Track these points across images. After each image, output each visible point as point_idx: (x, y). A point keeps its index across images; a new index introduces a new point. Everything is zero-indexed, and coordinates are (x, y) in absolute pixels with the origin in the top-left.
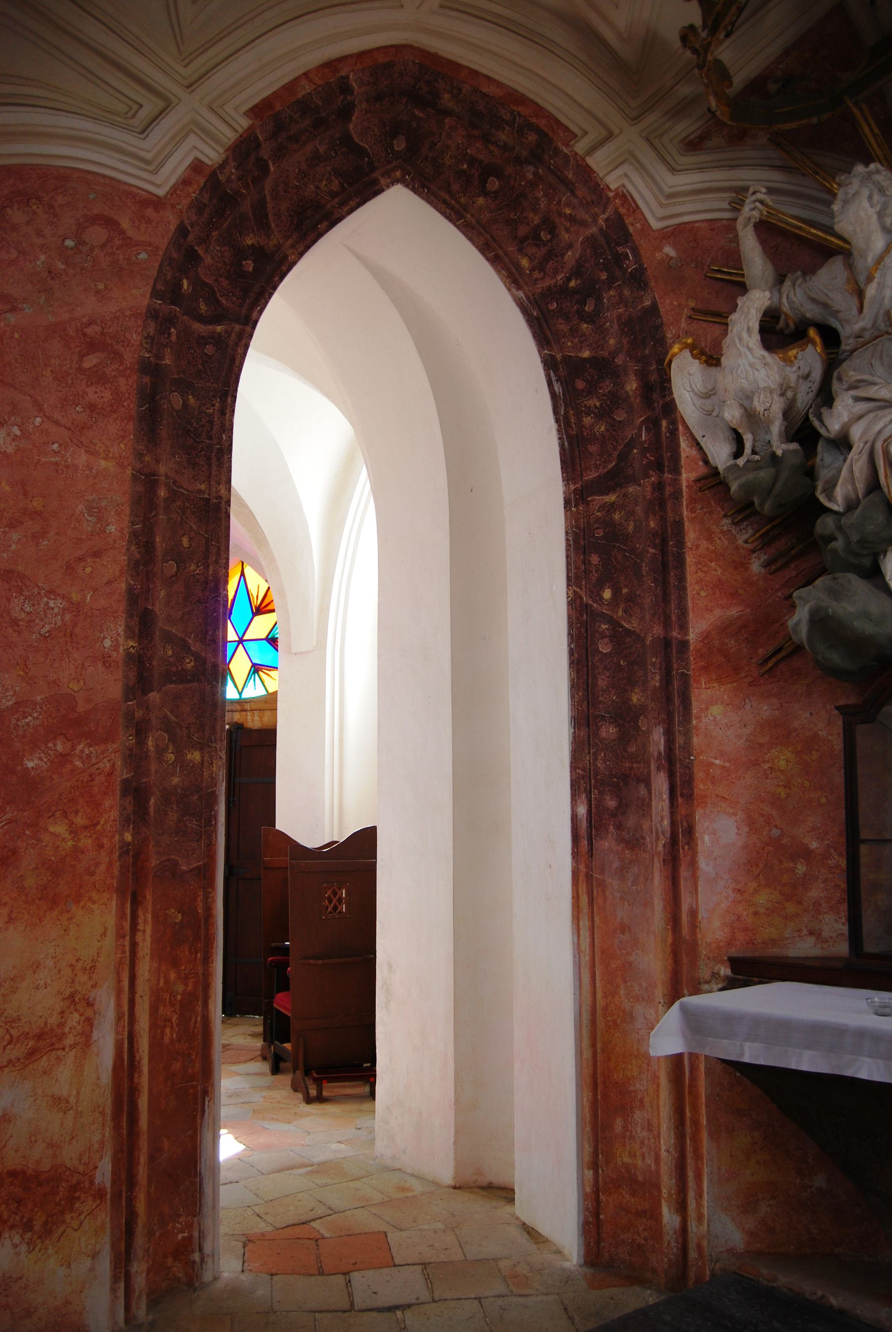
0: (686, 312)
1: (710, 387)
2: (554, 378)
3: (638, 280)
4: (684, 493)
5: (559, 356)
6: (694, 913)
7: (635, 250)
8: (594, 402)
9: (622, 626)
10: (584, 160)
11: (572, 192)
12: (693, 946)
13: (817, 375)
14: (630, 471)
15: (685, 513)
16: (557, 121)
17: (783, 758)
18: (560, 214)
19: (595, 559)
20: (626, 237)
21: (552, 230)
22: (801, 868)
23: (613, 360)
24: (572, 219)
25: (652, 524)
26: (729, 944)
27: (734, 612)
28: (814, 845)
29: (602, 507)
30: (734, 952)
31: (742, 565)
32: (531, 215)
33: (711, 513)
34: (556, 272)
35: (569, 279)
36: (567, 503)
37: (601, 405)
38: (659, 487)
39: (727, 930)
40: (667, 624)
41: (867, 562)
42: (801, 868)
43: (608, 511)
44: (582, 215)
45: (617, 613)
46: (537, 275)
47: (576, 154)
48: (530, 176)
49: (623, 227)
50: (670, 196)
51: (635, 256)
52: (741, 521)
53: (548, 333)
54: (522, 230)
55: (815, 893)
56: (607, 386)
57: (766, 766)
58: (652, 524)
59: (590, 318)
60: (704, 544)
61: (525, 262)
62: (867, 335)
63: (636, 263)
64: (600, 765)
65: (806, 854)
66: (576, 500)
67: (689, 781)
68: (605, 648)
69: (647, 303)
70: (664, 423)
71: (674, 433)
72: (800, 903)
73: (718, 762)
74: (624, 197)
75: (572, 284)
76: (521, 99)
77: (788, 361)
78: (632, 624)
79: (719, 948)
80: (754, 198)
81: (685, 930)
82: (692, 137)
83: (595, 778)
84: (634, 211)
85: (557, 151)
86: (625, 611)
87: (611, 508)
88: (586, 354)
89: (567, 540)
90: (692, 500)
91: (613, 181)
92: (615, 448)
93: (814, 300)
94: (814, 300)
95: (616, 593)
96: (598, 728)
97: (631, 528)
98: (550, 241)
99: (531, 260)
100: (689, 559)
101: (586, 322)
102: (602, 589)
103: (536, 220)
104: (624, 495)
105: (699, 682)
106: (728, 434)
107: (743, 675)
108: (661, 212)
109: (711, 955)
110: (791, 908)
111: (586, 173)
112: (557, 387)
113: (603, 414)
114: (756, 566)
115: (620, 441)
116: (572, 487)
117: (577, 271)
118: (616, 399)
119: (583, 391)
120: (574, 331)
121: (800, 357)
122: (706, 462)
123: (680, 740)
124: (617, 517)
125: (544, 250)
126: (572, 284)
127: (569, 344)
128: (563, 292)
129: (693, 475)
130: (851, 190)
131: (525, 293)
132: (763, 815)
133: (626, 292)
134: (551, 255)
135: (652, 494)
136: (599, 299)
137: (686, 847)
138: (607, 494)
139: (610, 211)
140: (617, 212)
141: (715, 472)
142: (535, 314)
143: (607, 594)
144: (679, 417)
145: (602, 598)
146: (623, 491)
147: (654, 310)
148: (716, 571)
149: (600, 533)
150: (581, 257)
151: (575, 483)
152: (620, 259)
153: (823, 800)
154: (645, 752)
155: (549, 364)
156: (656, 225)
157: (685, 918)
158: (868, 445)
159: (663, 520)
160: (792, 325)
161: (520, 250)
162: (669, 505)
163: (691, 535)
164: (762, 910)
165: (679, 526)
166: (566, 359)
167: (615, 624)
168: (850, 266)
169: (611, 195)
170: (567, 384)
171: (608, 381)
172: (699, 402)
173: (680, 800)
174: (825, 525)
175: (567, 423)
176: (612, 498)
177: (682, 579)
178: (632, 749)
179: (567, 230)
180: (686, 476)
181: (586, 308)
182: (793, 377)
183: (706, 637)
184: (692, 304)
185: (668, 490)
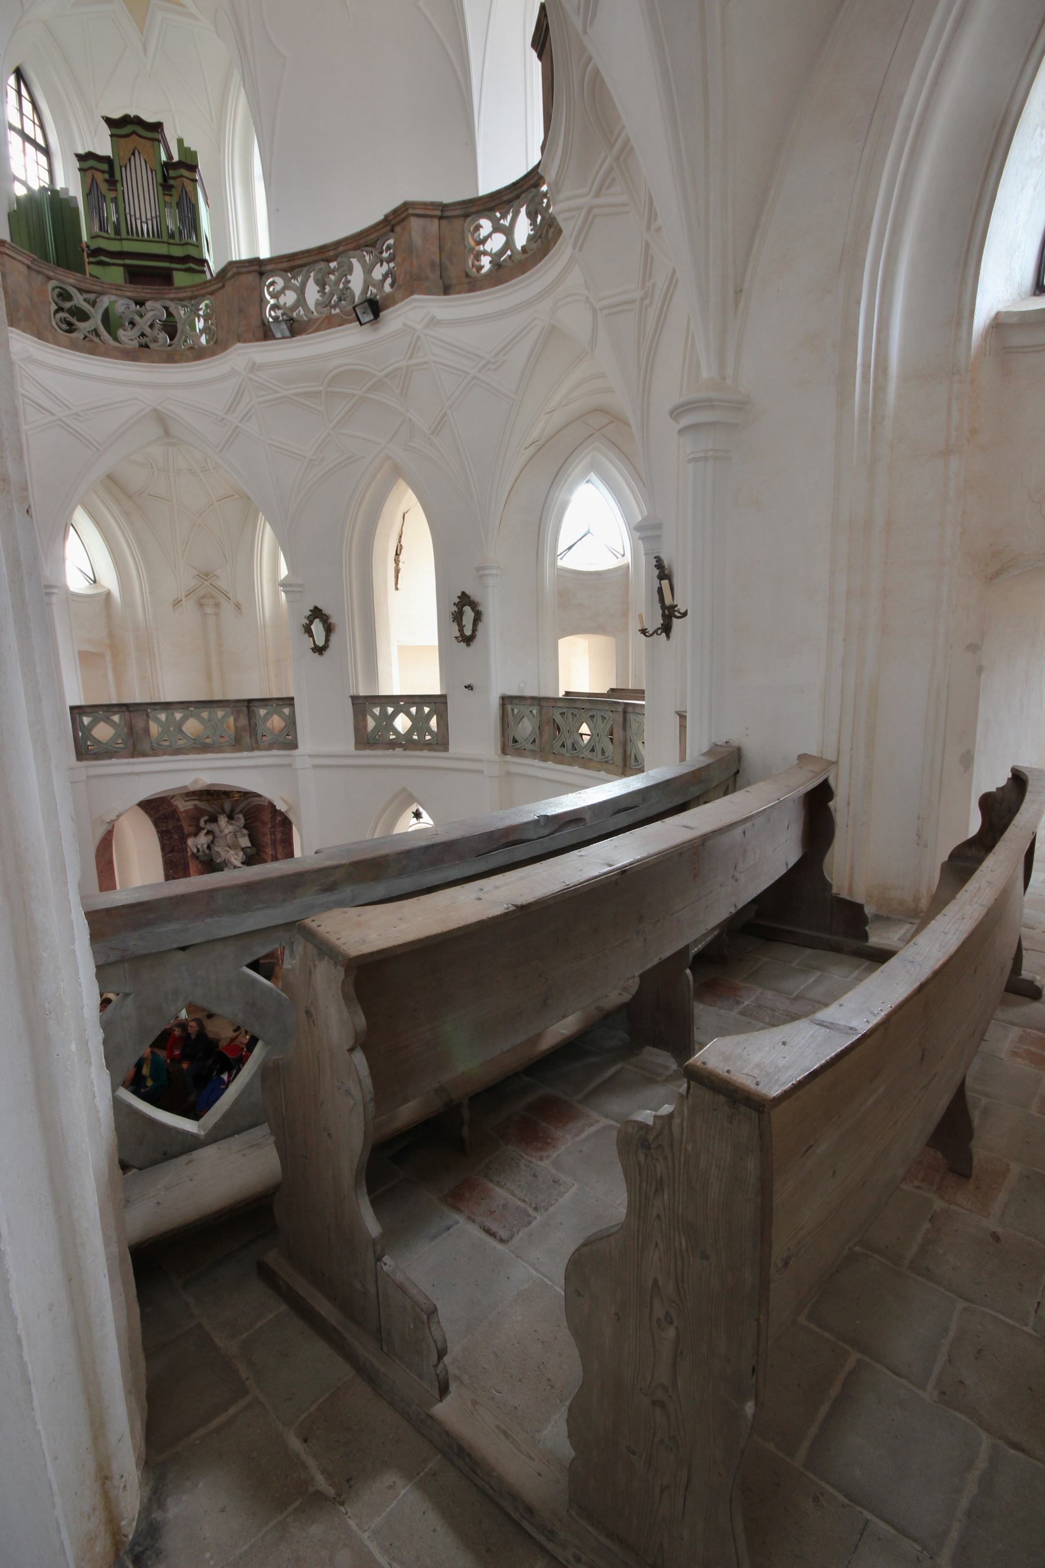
3: (178, 820)
7: (178, 815)
8: (166, 838)
13: (211, 839)
20: (176, 812)
59: (165, 823)
74: (176, 806)
87: (170, 857)
114: (200, 866)
143: (171, 872)
147: (182, 825)
155: (158, 832)
156: (181, 810)
163: (190, 864)
165: (188, 863)
170: (161, 835)
180: (189, 854)
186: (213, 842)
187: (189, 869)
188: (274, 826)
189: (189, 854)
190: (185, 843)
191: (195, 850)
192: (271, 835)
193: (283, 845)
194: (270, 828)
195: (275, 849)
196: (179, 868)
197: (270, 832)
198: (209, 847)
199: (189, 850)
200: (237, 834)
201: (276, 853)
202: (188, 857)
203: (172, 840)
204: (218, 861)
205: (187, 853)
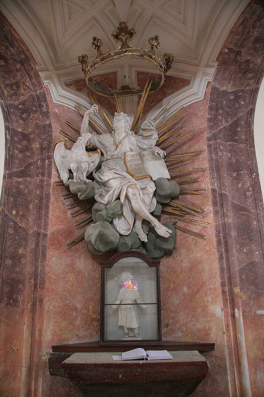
0: (59, 131)
1: (66, 156)
2: (7, 133)
4: (52, 186)
5: (11, 127)
6: (41, 331)
7: (47, 106)
8: (19, 146)
9: (18, 225)
10: (38, 72)
11: (30, 79)
12: (40, 343)
13: (97, 163)
14: (29, 173)
15: (51, 192)
16: (33, 57)
17: (71, 277)
18: (24, 84)
19: (11, 199)
20: (45, 100)
21: (18, 87)
22: (74, 314)
23: (29, 135)
24: (28, 87)
25: (38, 192)
26: (52, 341)
27: (61, 227)
28: (78, 306)
29: (16, 182)
30: (54, 344)
31: (66, 213)
32: (12, 79)
33: (58, 194)
34: (15, 101)
35: (19, 104)
36: (4, 177)
37: (22, 148)
38: (42, 181)
39: (52, 336)
40: (39, 227)
41: (110, 220)
42: (74, 314)
43: (18, 184)
44: (31, 87)
45: (17, 220)
46: (9, 98)
47: (36, 69)
48: (18, 67)
49: (45, 98)
50: (60, 95)
51: (46, 108)
52: (67, 199)
53: (9, 118)
54: (8, 82)
55: (78, 322)
56: (25, 143)
57: (67, 279)
58: (38, 192)
60: (56, 203)
61: (6, 92)
62: (115, 157)
63: (46, 110)
64: (4, 274)
65: (76, 309)
66: (8, 177)
67: (43, 283)
68: (11, 231)
69: (48, 123)
70: (47, 161)
71: (50, 165)
72: (73, 325)
73: (53, 277)
75: (20, 106)
76: (24, 44)
77: (90, 157)
78: (23, 225)
79: (49, 343)
80: (94, 108)
81: (37, 337)
82: (67, 83)
83: (2, 279)
84: (49, 95)
85: (30, 65)
86: (20, 220)
88: (20, 130)
89: (2, 190)
90: (53, 188)
91: (46, 82)
92: (24, 164)
93: (100, 142)
94: (100, 142)
95: (18, 212)
96: (5, 260)
97: (26, 191)
98: (16, 90)
99: (8, 92)
100: (51, 206)
101: (22, 120)
102: (12, 210)
103: (14, 81)
104: (25, 180)
105: (49, 248)
106: (68, 171)
107: (62, 248)
108: (57, 99)
109: (46, 346)
110: (71, 327)
111: (38, 76)
112: (8, 137)
113: (21, 151)
115: (26, 162)
116: (7, 172)
117: (23, 103)
118: (28, 148)
119: (16, 141)
120: (17, 121)
121: (93, 156)
122: (59, 177)
123: (40, 268)
124: (21, 186)
125: (13, 92)
126: (20, 106)
127: (15, 125)
128: (16, 107)
129: (55, 180)
130: (120, 118)
131: (4, 102)
132: (64, 296)
133: (40, 117)
134: (15, 94)
135: (39, 182)
136: (29, 115)
137: (40, 306)
138: (19, 178)
139: (42, 90)
140: (44, 92)
141: (62, 181)
142: (6, 110)
143: (14, 212)
144: (53, 161)
145: (12, 214)
146: (25, 179)
147: (50, 126)
148: (58, 213)
149: (14, 191)
150: (26, 100)
151: (9, 171)
152: (40, 106)
153: (81, 292)
154: (23, 271)
155: (7, 128)
157: (37, 333)
158: (122, 186)
159: (42, 192)
160: (91, 146)
161: (5, 88)
162: (45, 188)
163: (52, 199)
164: (62, 328)
165: (48, 196)
166: (13, 129)
167: (16, 223)
168: (113, 137)
169: (44, 86)
170: (12, 137)
171: (25, 142)
172: (61, 158)
173: (39, 289)
174: (96, 206)
175: (9, 150)
176: (20, 180)
177: (47, 213)
178: (17, 269)
179: (25, 90)
180: (54, 179)
181: (23, 116)
182: (90, 161)
183: (53, 234)
184: (61, 129)
185: (45, 183)
186: (99, 168)
187: (47, 207)
188: (214, 137)
189: (54, 179)
190: (50, 158)
191: (65, 176)
192: (210, 152)
193: (235, 175)
194: (209, 139)
195: (220, 178)
196: (31, 207)
197: (209, 146)
198: (90, 176)
199: (54, 172)
200: (145, 152)
201: (221, 186)
202: (49, 185)
203: (28, 154)
204: (106, 199)
205: (49, 176)
